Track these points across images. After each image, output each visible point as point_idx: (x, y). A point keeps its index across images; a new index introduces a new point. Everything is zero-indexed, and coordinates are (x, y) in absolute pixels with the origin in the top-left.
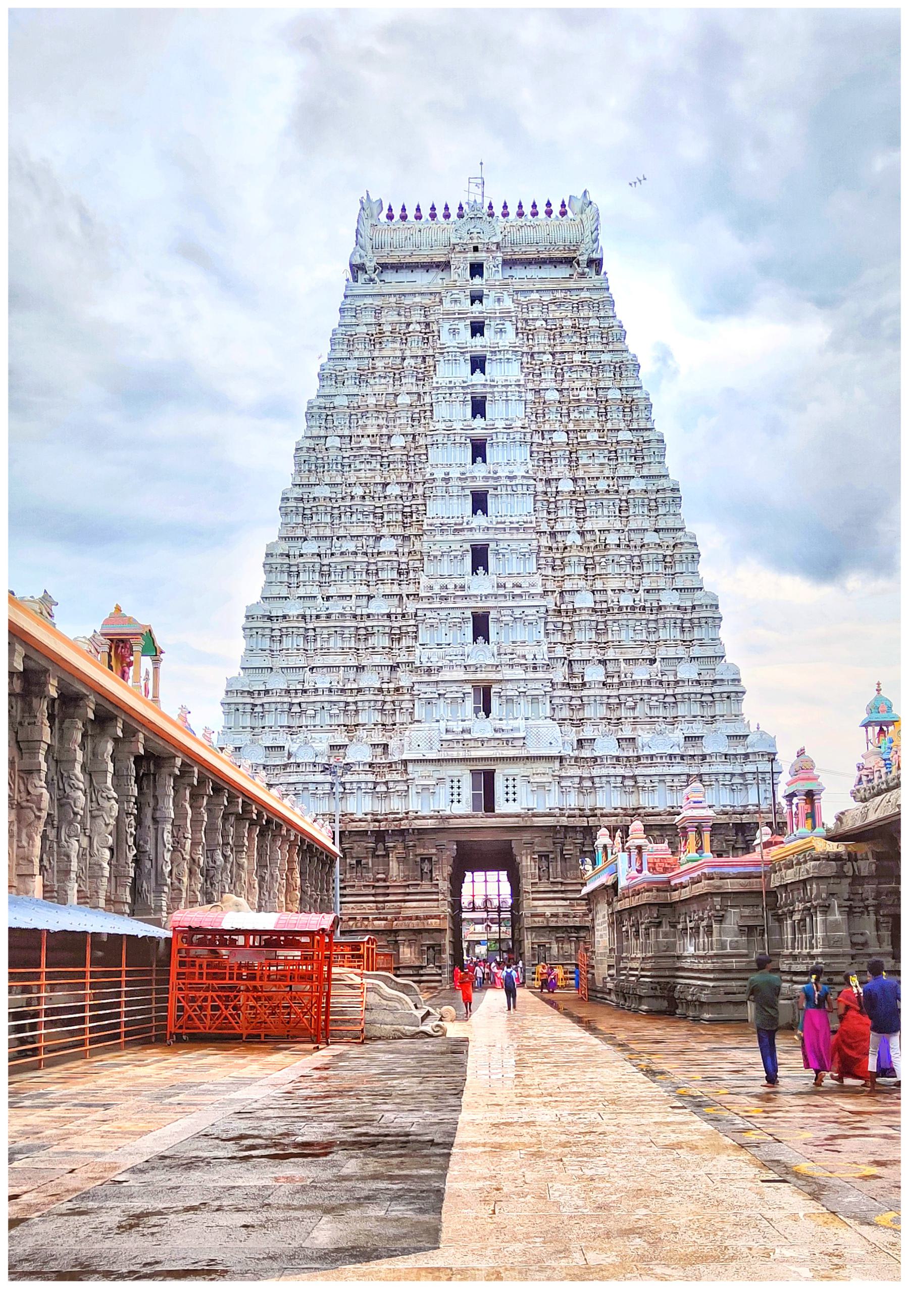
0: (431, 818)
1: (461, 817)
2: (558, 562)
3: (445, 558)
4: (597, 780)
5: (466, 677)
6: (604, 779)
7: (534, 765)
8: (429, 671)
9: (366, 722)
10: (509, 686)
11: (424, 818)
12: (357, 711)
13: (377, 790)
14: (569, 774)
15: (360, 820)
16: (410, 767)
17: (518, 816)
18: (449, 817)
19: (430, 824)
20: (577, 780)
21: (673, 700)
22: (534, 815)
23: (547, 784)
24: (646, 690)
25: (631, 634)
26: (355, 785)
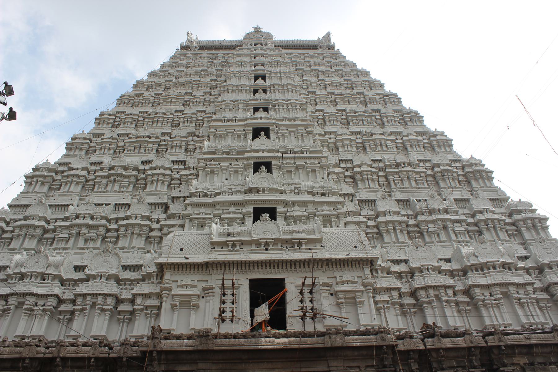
0: (189, 338)
1: (235, 337)
2: (332, 146)
3: (230, 136)
4: (422, 293)
5: (247, 197)
6: (432, 292)
7: (337, 274)
8: (205, 195)
9: (127, 245)
10: (296, 208)
11: (179, 337)
12: (118, 238)
13: (120, 309)
14: (384, 286)
15: (85, 345)
16: (167, 276)
17: (321, 335)
18: (216, 336)
19: (186, 345)
20: (395, 294)
21: (476, 228)
22: (347, 334)
23: (358, 295)
24: (447, 216)
25: (414, 184)
26: (89, 298)
